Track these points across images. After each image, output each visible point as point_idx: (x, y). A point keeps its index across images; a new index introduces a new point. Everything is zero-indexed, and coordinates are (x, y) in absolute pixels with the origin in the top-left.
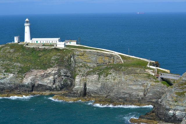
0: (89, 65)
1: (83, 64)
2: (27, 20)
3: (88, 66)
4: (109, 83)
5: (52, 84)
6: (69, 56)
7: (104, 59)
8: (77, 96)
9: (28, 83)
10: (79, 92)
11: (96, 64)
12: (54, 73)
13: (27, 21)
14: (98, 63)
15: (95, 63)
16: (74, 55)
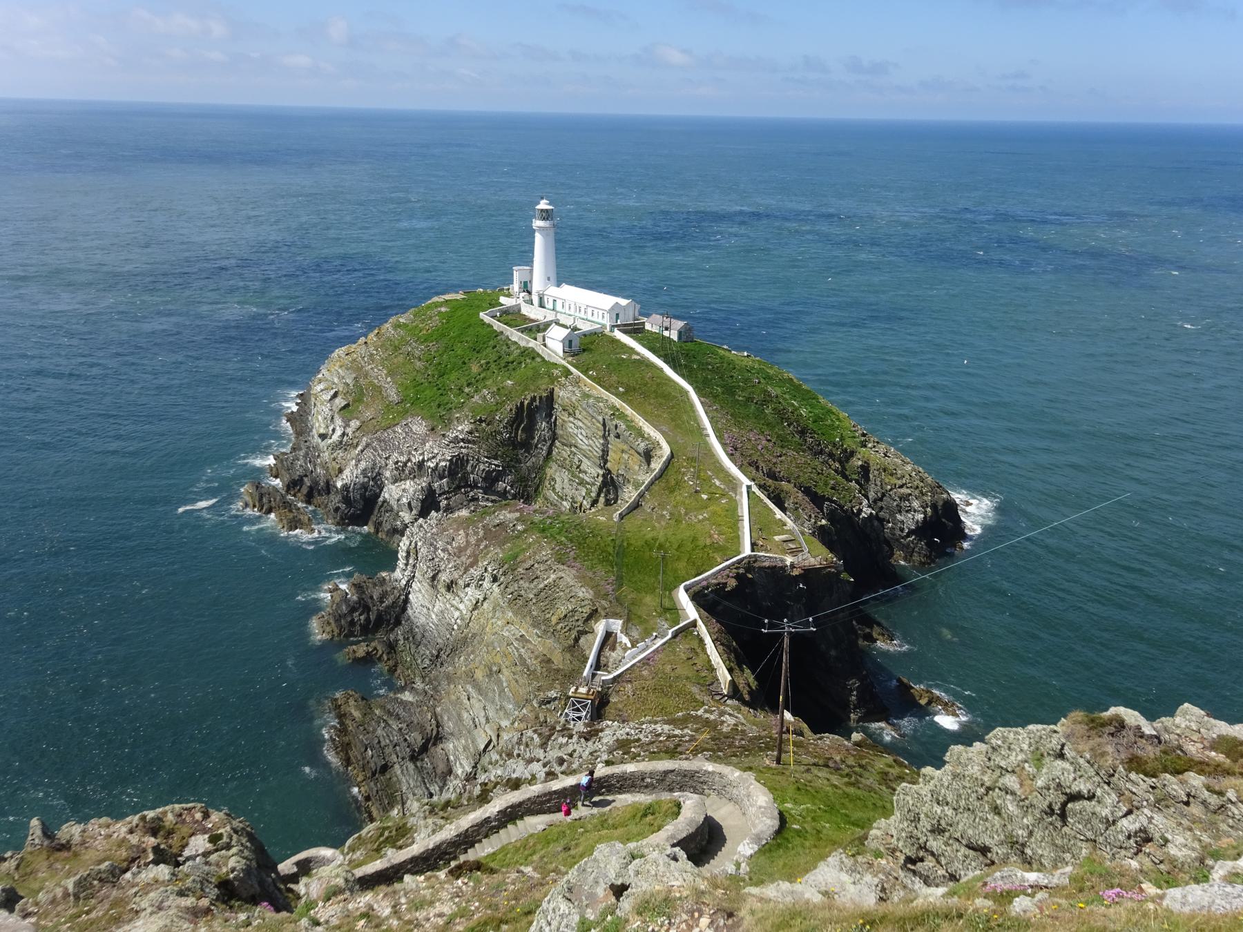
0: (586, 465)
1: (571, 452)
2: (543, 205)
3: (580, 471)
4: (457, 614)
5: (414, 512)
6: (526, 402)
7: (625, 456)
8: (352, 623)
9: (346, 487)
10: (387, 603)
11: (601, 472)
12: (435, 469)
13: (542, 210)
14: (609, 472)
15: (601, 468)
16: (550, 399)
